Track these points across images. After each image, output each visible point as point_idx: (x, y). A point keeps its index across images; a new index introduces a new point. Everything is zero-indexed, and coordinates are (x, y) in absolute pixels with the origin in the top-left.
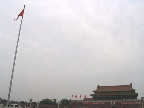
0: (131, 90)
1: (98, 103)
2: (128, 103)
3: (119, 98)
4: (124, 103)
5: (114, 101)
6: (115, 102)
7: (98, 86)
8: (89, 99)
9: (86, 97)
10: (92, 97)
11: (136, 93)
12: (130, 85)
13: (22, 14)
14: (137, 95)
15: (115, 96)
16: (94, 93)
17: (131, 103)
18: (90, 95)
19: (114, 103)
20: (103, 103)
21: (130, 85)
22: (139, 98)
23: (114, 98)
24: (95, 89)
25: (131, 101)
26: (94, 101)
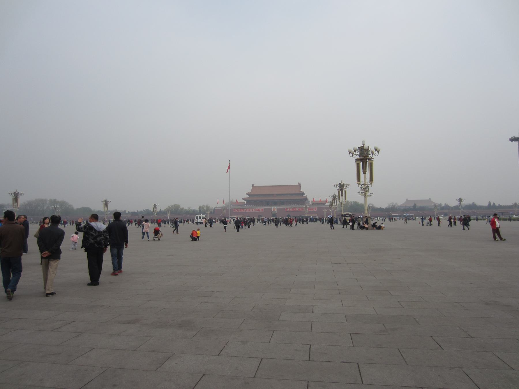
0: (299, 193)
1: (254, 210)
2: (293, 209)
3: (282, 202)
7: (253, 185)
8: (241, 205)
13: (229, 168)
16: (248, 196)
17: (297, 210)
18: (243, 199)
19: (276, 210)
23: (275, 203)
26: (248, 208)
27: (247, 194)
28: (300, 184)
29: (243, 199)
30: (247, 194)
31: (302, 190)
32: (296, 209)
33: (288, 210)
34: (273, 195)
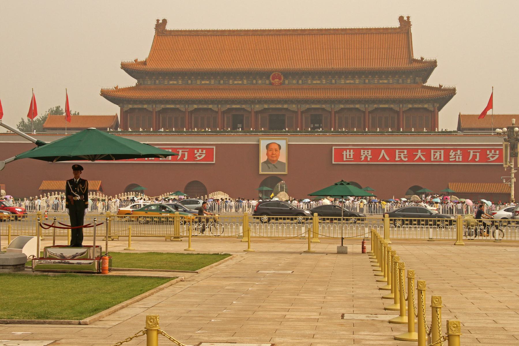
0: (404, 65)
2: (376, 152)
3: (316, 119)
5: (283, 143)
6: (289, 146)
9: (72, 113)
10: (115, 110)
11: (440, 88)
12: (397, 24)
14: (446, 95)
15: (293, 107)
16: (133, 82)
17: (401, 157)
19: (283, 158)
21: (397, 24)
22: (447, 119)
23: (276, 123)
24: (141, 51)
25: (401, 143)
27: (127, 68)
28: (405, 24)
29: (106, 94)
30: (127, 68)
31: (420, 51)
32: (391, 152)
33: (348, 155)
34: (265, 74)
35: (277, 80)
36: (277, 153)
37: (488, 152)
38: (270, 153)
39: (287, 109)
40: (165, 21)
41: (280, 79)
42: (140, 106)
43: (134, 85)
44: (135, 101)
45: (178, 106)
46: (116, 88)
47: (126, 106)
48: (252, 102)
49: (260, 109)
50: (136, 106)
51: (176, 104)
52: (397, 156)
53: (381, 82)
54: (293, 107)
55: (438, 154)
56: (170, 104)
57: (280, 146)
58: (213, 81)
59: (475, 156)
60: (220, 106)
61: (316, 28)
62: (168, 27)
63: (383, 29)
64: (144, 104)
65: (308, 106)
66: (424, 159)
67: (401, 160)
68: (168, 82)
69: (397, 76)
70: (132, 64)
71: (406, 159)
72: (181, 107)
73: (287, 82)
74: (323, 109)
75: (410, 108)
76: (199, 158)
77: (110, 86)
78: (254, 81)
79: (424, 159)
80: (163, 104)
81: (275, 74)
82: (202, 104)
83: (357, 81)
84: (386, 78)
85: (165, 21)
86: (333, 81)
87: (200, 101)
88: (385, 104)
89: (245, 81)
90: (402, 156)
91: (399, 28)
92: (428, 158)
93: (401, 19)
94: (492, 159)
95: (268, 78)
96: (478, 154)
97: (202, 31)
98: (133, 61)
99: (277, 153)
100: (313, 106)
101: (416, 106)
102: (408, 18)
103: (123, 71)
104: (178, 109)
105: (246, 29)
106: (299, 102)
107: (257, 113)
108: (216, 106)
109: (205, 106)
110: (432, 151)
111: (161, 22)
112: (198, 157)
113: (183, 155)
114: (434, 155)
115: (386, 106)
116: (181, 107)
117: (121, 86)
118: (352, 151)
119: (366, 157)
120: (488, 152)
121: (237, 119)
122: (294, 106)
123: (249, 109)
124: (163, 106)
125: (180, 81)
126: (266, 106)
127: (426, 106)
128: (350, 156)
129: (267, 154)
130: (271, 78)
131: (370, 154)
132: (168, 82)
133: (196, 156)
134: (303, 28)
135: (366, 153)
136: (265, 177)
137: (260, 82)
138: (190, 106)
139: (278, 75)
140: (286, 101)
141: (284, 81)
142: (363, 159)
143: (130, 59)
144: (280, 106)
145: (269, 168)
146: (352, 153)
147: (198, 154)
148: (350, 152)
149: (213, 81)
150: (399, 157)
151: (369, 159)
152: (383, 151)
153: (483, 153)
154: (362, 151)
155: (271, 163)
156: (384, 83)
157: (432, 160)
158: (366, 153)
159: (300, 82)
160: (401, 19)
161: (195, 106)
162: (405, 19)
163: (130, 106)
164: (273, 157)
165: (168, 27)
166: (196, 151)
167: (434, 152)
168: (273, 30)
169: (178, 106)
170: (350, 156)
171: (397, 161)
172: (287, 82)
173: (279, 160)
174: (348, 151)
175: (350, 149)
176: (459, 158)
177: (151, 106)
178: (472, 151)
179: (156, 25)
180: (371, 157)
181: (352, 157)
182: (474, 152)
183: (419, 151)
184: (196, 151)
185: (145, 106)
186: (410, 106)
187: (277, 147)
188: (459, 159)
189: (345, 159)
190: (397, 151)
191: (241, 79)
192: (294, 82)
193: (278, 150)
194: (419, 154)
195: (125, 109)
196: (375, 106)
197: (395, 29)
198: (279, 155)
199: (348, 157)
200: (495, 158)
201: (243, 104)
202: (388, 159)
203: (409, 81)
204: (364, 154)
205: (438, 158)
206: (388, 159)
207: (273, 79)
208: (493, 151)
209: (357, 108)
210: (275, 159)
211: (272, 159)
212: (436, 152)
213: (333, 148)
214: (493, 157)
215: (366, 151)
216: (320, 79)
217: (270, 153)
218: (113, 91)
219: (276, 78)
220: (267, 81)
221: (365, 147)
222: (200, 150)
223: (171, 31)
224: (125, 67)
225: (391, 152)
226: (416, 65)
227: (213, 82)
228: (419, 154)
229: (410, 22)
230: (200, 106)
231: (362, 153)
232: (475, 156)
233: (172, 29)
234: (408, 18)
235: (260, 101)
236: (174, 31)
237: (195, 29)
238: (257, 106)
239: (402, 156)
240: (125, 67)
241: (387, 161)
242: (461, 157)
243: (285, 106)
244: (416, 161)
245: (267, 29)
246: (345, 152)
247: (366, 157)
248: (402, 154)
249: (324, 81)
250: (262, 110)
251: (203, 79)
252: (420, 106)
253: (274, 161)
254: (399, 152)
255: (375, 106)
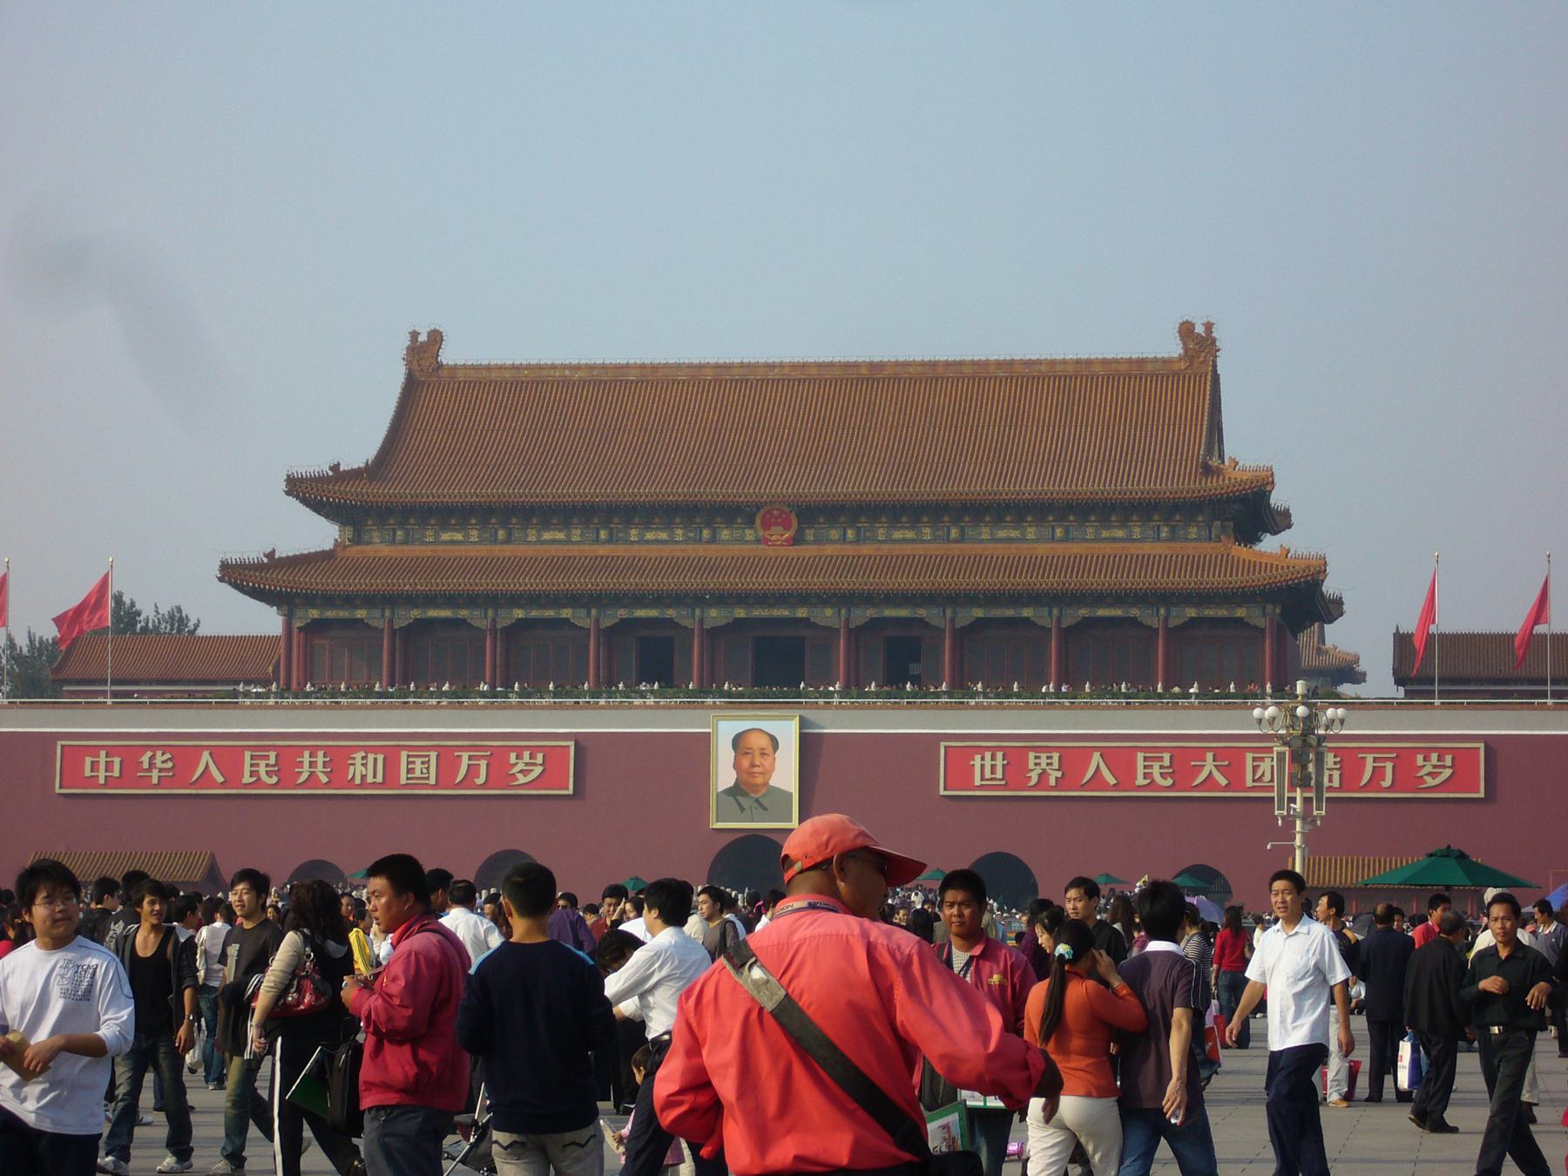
1: (420, 771)
3: (897, 656)
4: (986, 770)
5: (787, 730)
15: (827, 615)
17: (1152, 775)
18: (237, 575)
19: (785, 774)
20: (525, 772)
24: (356, 439)
28: (1200, 345)
29: (237, 575)
35: (774, 529)
36: (767, 764)
37: (1420, 759)
38: (746, 763)
39: (807, 620)
40: (436, 338)
41: (787, 527)
42: (343, 614)
43: (328, 545)
44: (329, 600)
45: (463, 613)
46: (271, 555)
47: (299, 613)
48: (697, 599)
49: (724, 622)
50: (330, 614)
51: (459, 607)
52: (1140, 771)
53: (1105, 534)
54: (827, 615)
55: (1265, 766)
56: (437, 607)
57: (774, 742)
58: (578, 532)
59: (1378, 773)
60: (594, 612)
61: (918, 359)
62: (448, 356)
63: (1130, 361)
64: (356, 607)
65: (871, 613)
66: (1223, 781)
67: (1152, 785)
68: (437, 535)
69: (1156, 517)
70: (320, 480)
71: (1169, 782)
72: (477, 618)
73: (810, 534)
74: (922, 622)
75: (1192, 619)
76: (522, 779)
77: (251, 550)
78: (706, 533)
79: (1223, 781)
80: (416, 606)
81: (770, 512)
82: (542, 607)
83: (1031, 533)
84: (1124, 523)
85: (436, 338)
86: (954, 533)
87: (534, 599)
88: (1112, 606)
89: (679, 532)
90: (1156, 771)
91: (1180, 359)
92: (1236, 780)
93: (1186, 330)
94: (1430, 782)
95: (750, 522)
96: (1389, 766)
97: (553, 367)
98: (326, 468)
99: (770, 759)
100: (890, 612)
101: (1210, 612)
102: (1209, 327)
103: (293, 502)
104: (462, 623)
105: (696, 361)
106: (846, 599)
107: (714, 635)
108: (582, 612)
109: (550, 613)
110: (1249, 756)
111: (423, 338)
112: (520, 776)
113: (472, 771)
114: (1255, 769)
115: (1117, 612)
116: (477, 618)
117: (287, 548)
118: (999, 755)
119: (1043, 775)
120: (1420, 759)
121: (649, 655)
122: (829, 612)
123: (688, 623)
124: (415, 613)
125: (475, 533)
126: (741, 613)
127: (1240, 612)
128: (993, 767)
129: (736, 766)
130: (758, 522)
131: (1056, 766)
132: (437, 535)
133: (514, 770)
134: (876, 359)
135: (1044, 761)
136: (727, 840)
137: (725, 534)
138: (503, 612)
139: (782, 512)
140: (803, 598)
141: (800, 530)
142: (1033, 782)
143: (315, 463)
144: (784, 613)
145: (742, 809)
146: (1000, 762)
147: (521, 766)
148: (993, 758)
149: (578, 532)
150: (1146, 776)
151: (1052, 782)
152: (1096, 757)
153: (1404, 760)
154: (1032, 755)
155: (745, 794)
156: (1114, 540)
157: (1249, 783)
158: (1044, 761)
159: (850, 534)
160: (1186, 330)
161: (519, 613)
162: (1200, 329)
163: (314, 613)
164: (752, 774)
165: (448, 356)
166: (513, 756)
167: (1254, 759)
168: (781, 365)
169: (463, 613)
170: (993, 767)
171: (1140, 788)
172: (810, 534)
173: (771, 783)
174: (988, 755)
175: (994, 750)
176: (1331, 780)
177: (377, 613)
178: (1370, 758)
179: (408, 348)
180: (1059, 774)
181: (999, 775)
182: (1375, 760)
183: (1210, 756)
184: (513, 756)
185: (361, 614)
186: (1191, 612)
187: (764, 742)
188: (1331, 780)
189: (978, 782)
190: (1140, 756)
191: (668, 526)
192: (834, 534)
193: (769, 750)
194: (1209, 765)
195: (298, 624)
196: (1084, 612)
197: (1166, 361)
198: (772, 768)
199: (988, 775)
200: (1438, 781)
201: (669, 606)
202: (1112, 781)
203: (1193, 532)
204: (1037, 765)
205: (1267, 777)
206: (1112, 781)
207: (766, 525)
208: (1434, 756)
209: (1026, 620)
210: (759, 780)
211: (750, 780)
212: (1262, 759)
213: (943, 744)
214: (1432, 775)
215: (1044, 756)
216: (915, 523)
217: (746, 763)
218: (257, 567)
219: (776, 524)
220: (748, 532)
221: (1040, 743)
222: (526, 754)
223: (455, 368)
224: (301, 488)
225: (1120, 756)
226: (1212, 485)
227: (576, 534)
228: (1209, 765)
229: (1214, 341)
230: (534, 613)
231: (1031, 761)
232: (1378, 773)
233: (460, 362)
234: (1209, 327)
235: (722, 599)
236: (465, 367)
237: (533, 362)
238: (713, 612)
239: (1156, 771)
240: (301, 488)
241: (1105, 786)
242: (1336, 774)
243: (801, 613)
244: (1196, 788)
245: (762, 361)
246: (978, 758)
247: (1043, 775)
248: (1156, 765)
249: (928, 530)
250: (727, 625)
251: (546, 525)
252: (1223, 613)
253: (755, 788)
254: (1145, 759)
255: (1084, 612)
